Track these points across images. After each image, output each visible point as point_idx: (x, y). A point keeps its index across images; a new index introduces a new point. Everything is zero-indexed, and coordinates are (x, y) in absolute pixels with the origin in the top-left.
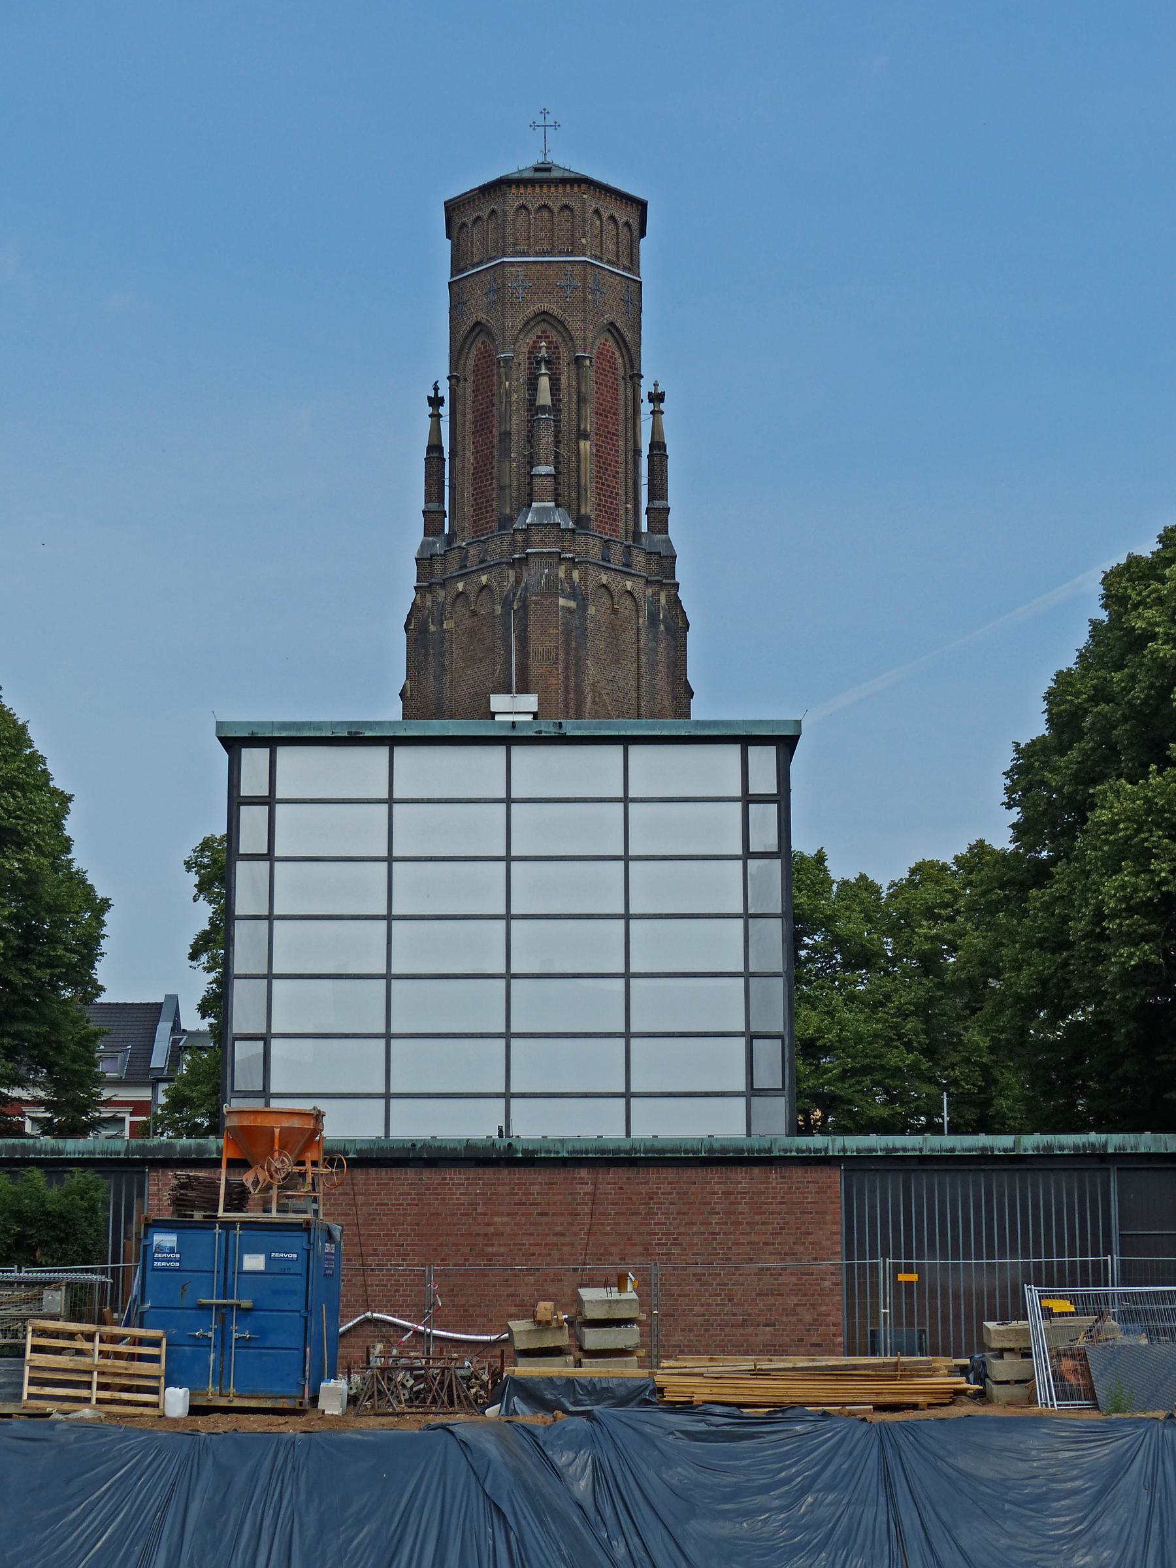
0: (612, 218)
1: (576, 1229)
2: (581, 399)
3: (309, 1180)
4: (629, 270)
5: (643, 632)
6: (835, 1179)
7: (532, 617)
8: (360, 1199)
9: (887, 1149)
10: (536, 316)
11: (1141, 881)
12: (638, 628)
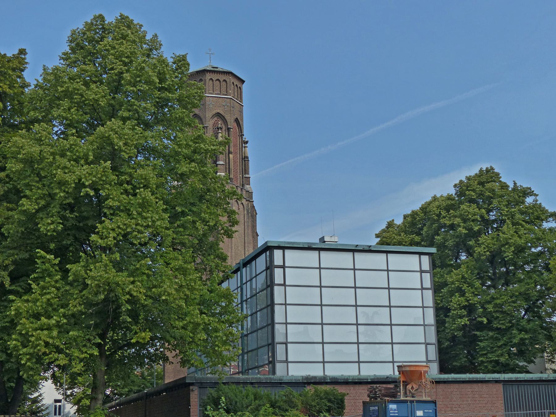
0: (236, 85)
4: (241, 102)
5: (245, 216)
6: (501, 386)
9: (515, 378)
11: (462, 299)
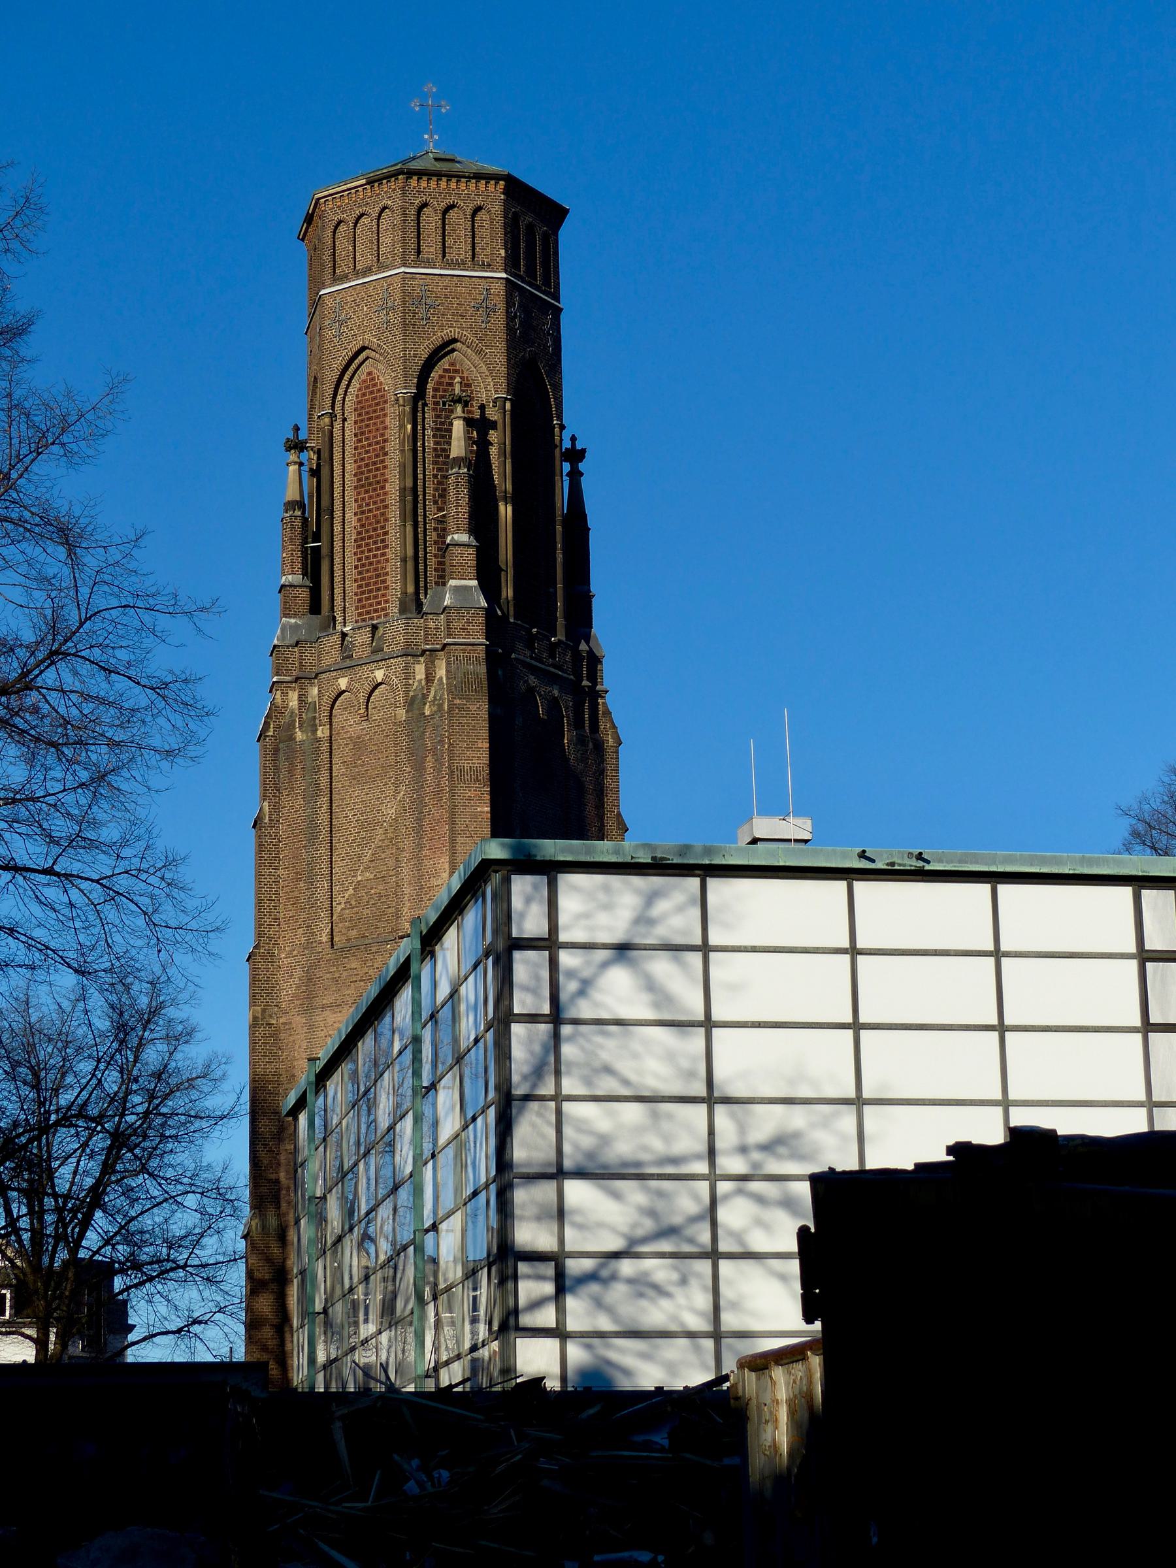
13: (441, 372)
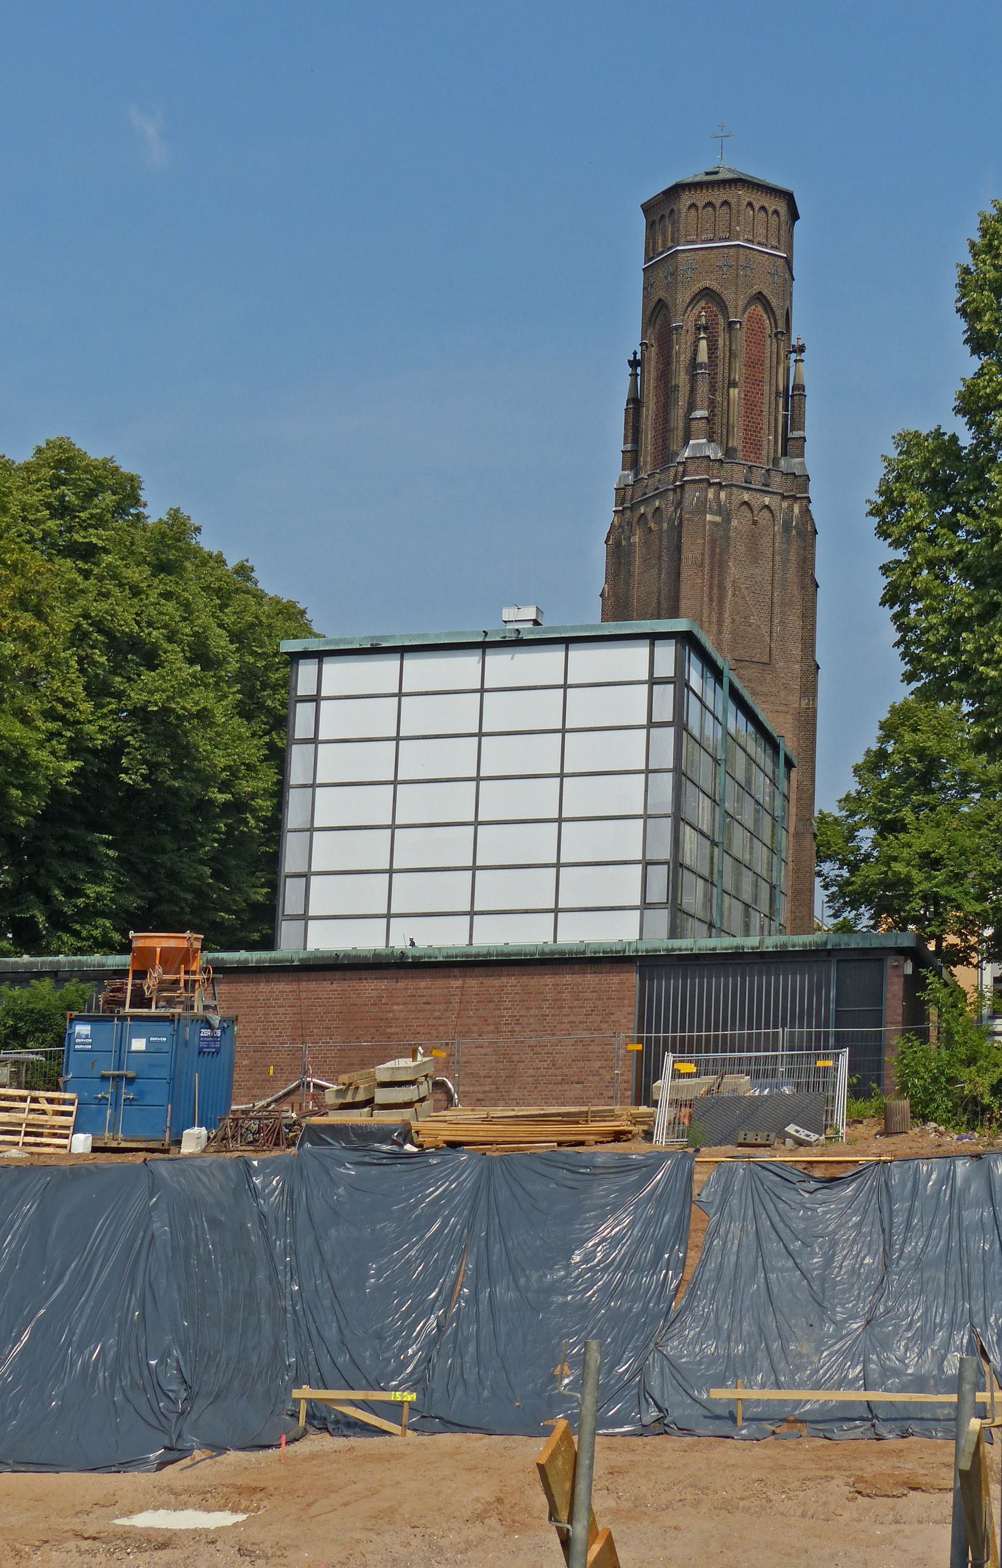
1: (449, 1014)
2: (732, 355)
3: (182, 984)
7: (684, 531)
8: (303, 995)
9: (667, 950)
10: (701, 291)
12: (774, 535)
13: (700, 309)
